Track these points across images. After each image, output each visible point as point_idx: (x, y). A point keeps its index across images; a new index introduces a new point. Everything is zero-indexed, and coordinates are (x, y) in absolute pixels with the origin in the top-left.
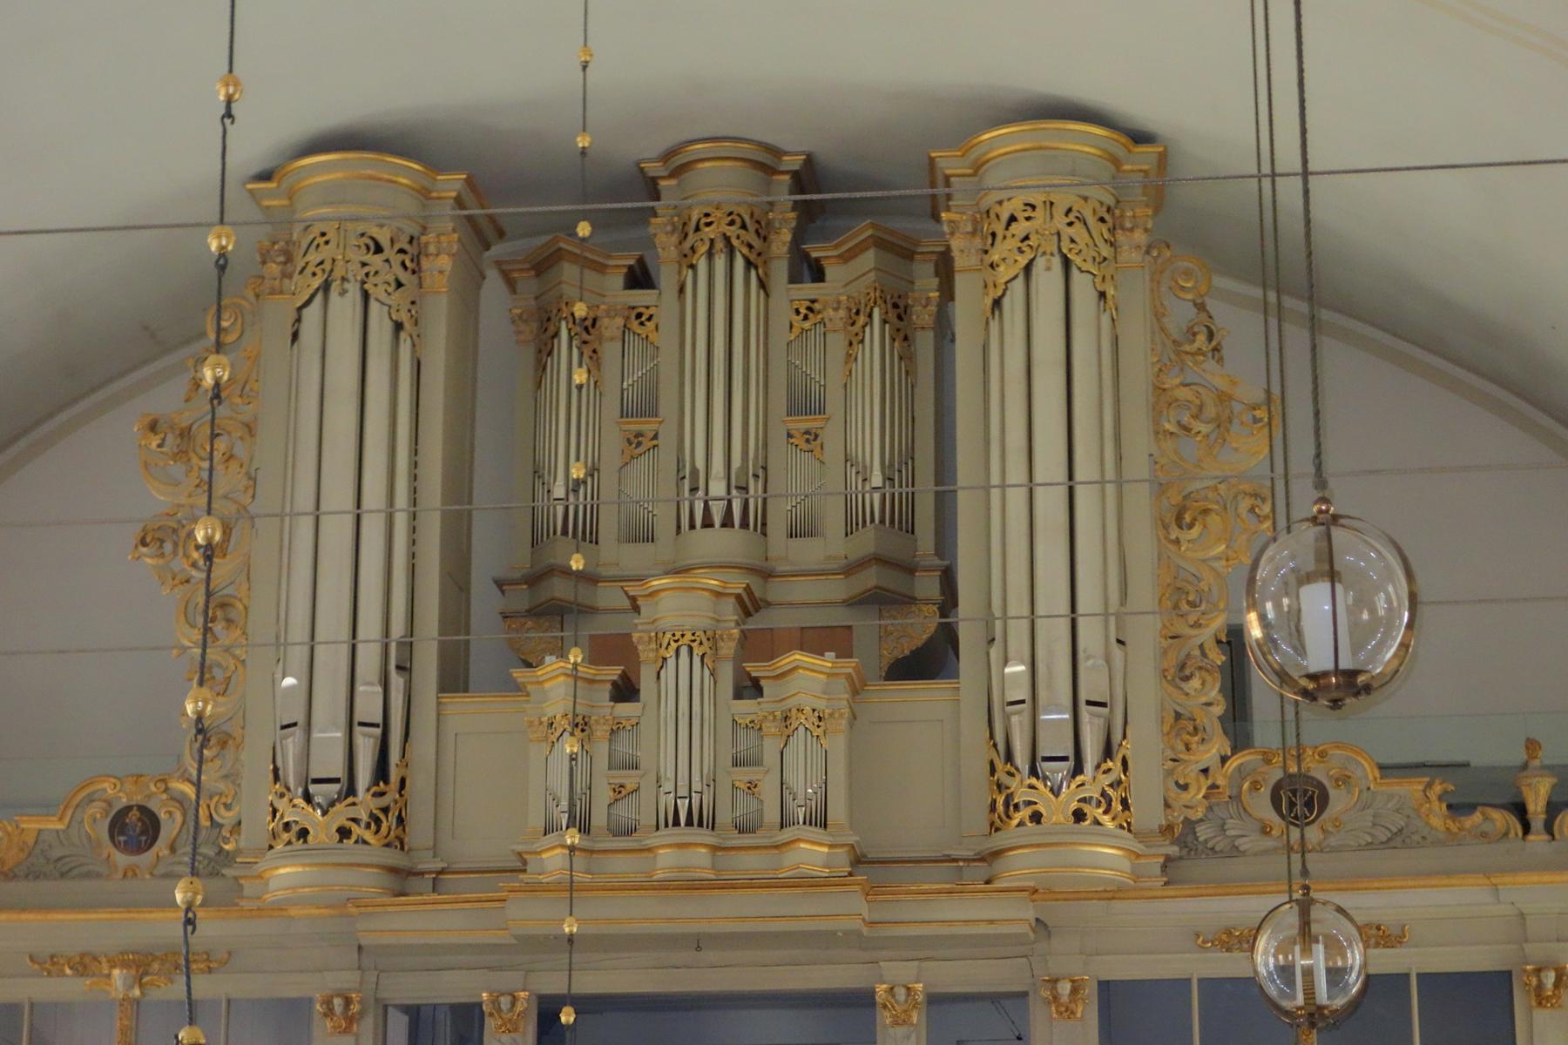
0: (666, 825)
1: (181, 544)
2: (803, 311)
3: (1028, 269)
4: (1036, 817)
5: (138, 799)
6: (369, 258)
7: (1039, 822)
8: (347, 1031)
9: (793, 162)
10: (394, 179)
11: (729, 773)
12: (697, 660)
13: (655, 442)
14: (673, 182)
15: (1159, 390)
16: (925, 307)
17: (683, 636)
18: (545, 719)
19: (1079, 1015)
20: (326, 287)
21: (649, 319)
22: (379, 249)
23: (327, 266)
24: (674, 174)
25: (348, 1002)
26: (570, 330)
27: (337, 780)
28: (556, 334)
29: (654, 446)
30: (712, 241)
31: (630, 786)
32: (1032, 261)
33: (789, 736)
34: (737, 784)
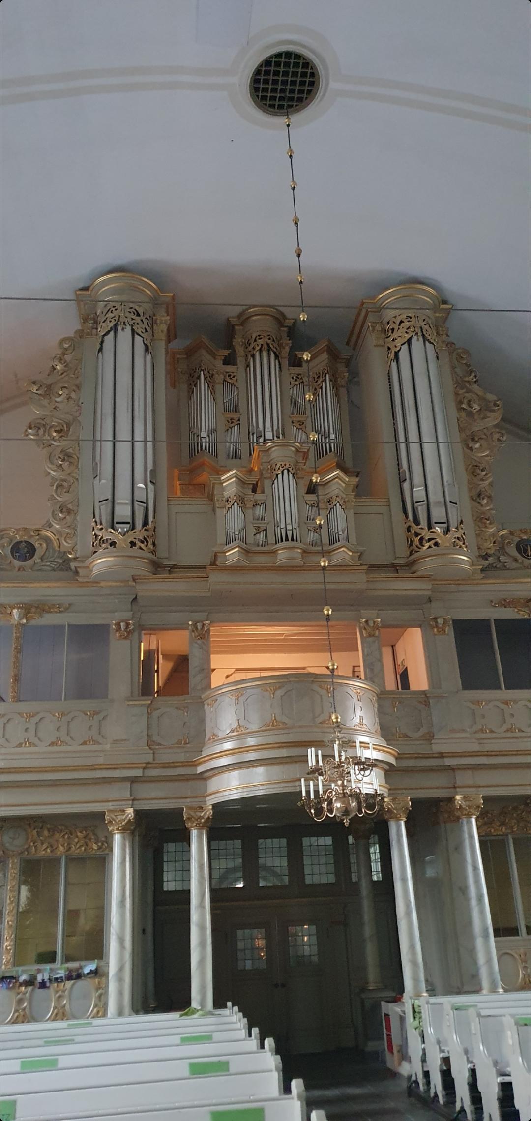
0: (282, 541)
1: (47, 431)
2: (295, 377)
3: (409, 342)
4: (436, 544)
5: (25, 538)
6: (134, 317)
7: (438, 546)
8: (126, 638)
9: (289, 323)
10: (144, 289)
11: (305, 523)
12: (291, 476)
13: (238, 422)
14: (241, 328)
15: (457, 394)
16: (343, 378)
17: (285, 465)
18: (224, 499)
19: (447, 633)
20: (116, 326)
21: (234, 377)
22: (138, 315)
23: (117, 318)
24: (242, 325)
25: (128, 625)
26: (204, 375)
27: (128, 523)
28: (199, 377)
29: (238, 424)
30: (262, 345)
31: (263, 527)
32: (411, 338)
33: (331, 509)
34: (309, 528)
